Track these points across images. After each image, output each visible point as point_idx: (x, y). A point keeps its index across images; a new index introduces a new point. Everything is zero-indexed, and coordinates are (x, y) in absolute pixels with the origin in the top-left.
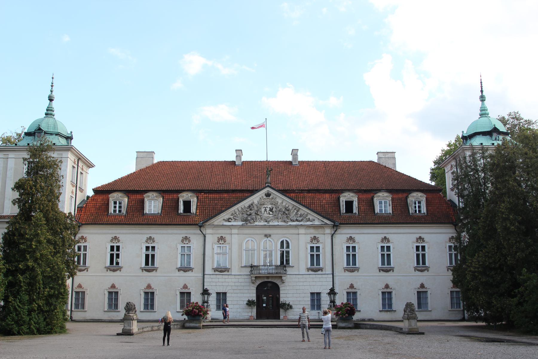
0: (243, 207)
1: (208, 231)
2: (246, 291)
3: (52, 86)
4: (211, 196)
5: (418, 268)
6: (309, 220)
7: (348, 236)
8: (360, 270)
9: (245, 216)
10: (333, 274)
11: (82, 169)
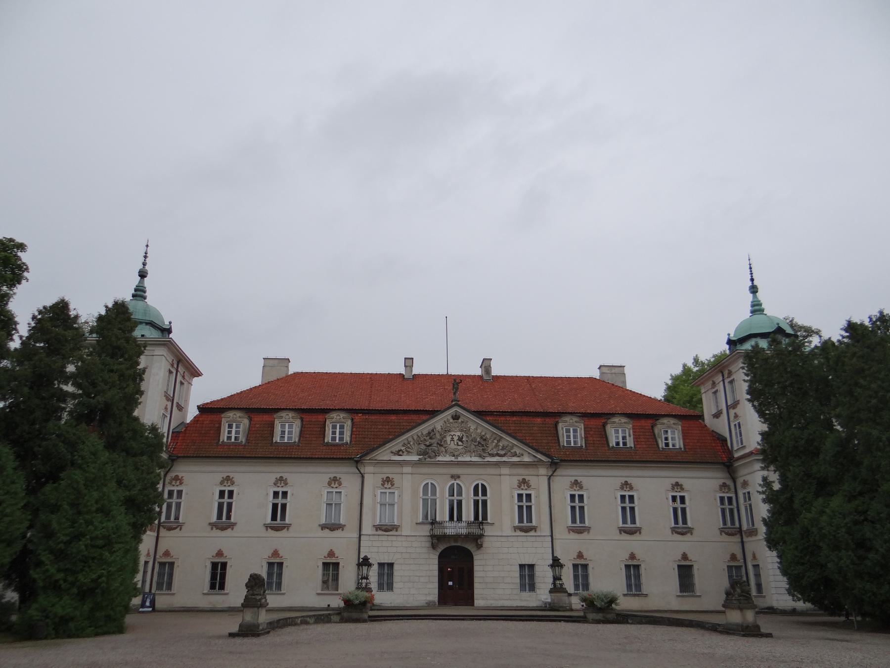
0: (420, 434)
1: (368, 469)
3: (145, 257)
4: (373, 417)
5: (679, 530)
6: (515, 455)
7: (573, 479)
8: (591, 531)
9: (423, 447)
10: (552, 536)
11: (183, 377)
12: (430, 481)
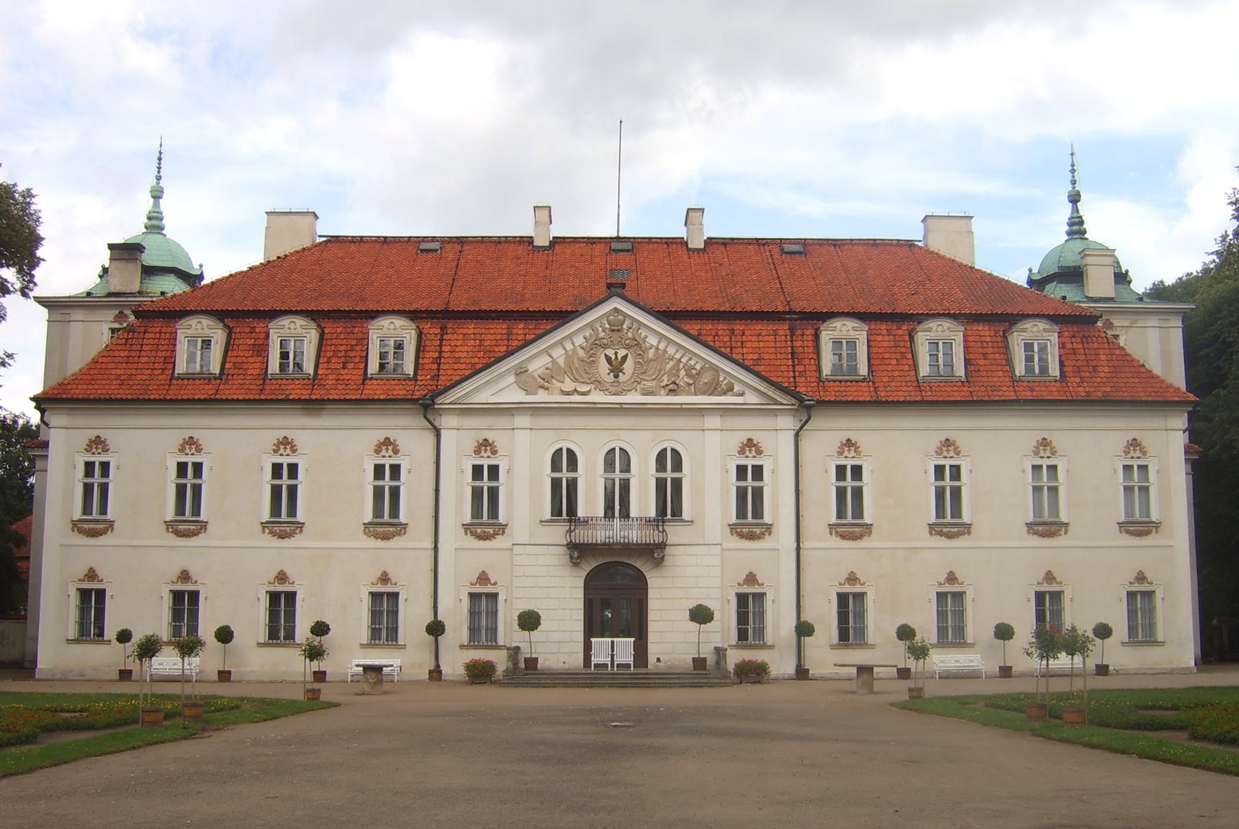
1: (447, 422)
12: (565, 445)
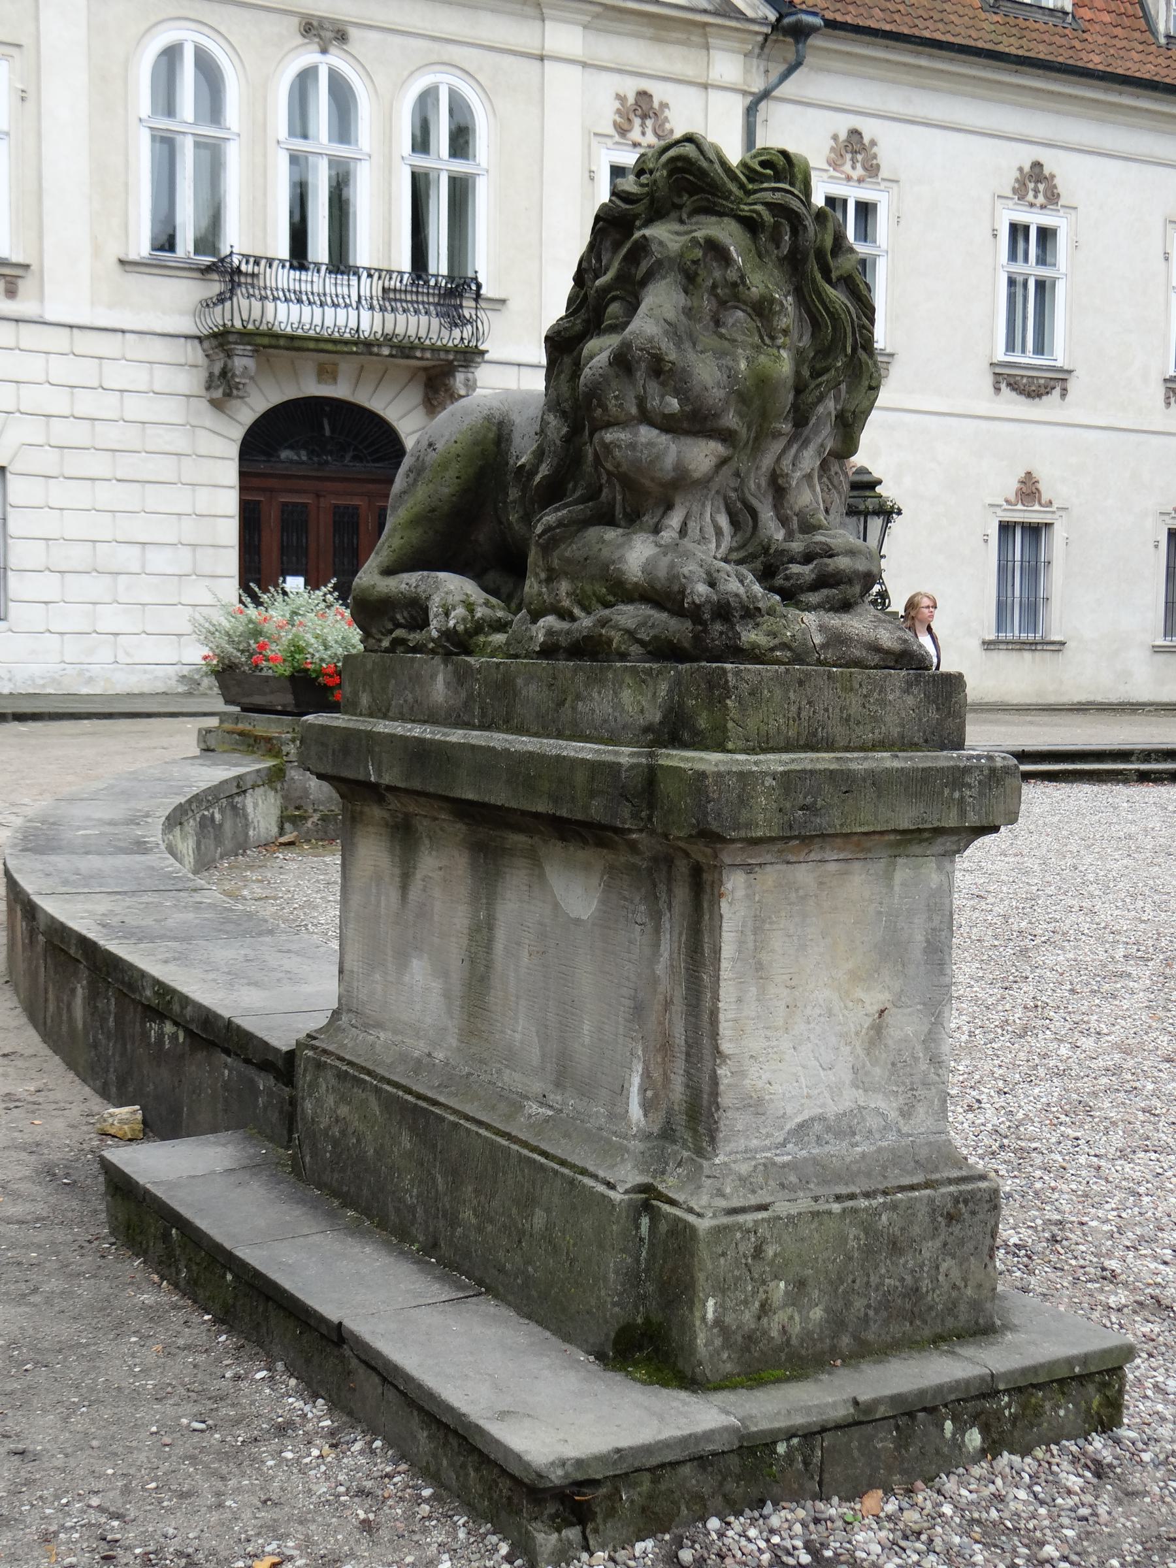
2: (163, 468)
